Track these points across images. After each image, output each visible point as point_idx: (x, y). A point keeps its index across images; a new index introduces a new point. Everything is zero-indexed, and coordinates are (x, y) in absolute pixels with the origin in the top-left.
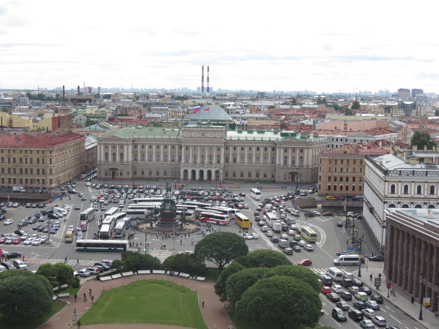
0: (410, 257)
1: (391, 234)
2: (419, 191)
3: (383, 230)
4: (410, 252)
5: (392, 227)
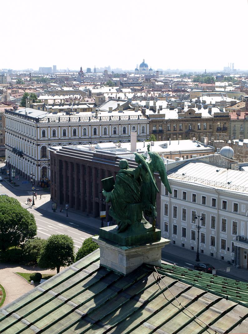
0: (81, 182)
1: (59, 167)
2: (64, 134)
3: (38, 168)
4: (81, 178)
5: (61, 161)
